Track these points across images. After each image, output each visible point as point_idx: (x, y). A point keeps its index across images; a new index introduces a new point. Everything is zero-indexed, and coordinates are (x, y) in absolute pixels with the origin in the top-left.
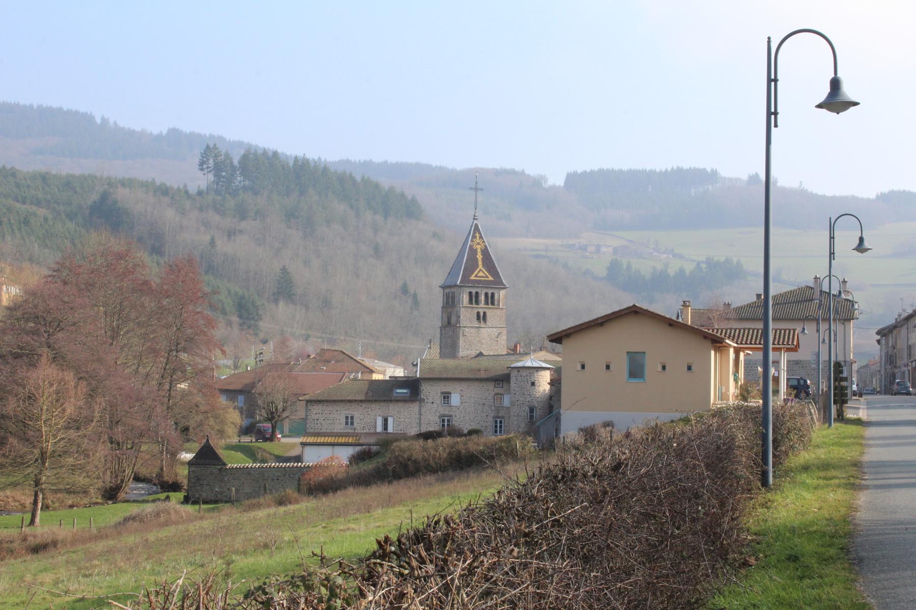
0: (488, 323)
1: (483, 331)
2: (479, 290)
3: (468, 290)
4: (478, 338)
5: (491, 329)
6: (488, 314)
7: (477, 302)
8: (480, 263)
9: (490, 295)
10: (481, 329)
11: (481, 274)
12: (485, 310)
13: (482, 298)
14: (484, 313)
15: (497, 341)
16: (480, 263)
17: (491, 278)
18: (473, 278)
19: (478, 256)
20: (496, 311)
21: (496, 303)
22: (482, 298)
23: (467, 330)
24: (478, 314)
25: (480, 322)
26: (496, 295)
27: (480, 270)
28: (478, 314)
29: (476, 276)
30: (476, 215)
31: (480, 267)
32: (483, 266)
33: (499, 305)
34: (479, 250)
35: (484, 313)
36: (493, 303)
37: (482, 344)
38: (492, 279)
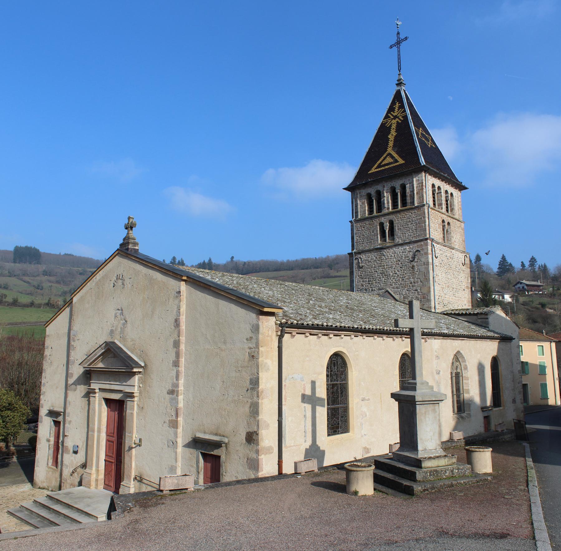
0: (398, 240)
1: (389, 253)
2: (379, 187)
3: (364, 192)
4: (381, 269)
5: (401, 249)
6: (395, 224)
7: (380, 207)
8: (391, 144)
9: (398, 191)
10: (385, 252)
11: (389, 160)
12: (391, 217)
13: (387, 199)
14: (391, 223)
15: (413, 267)
16: (391, 144)
17: (401, 161)
18: (373, 170)
19: (389, 137)
20: (408, 214)
21: (408, 199)
22: (387, 199)
23: (363, 256)
24: (382, 225)
25: (385, 241)
26: (408, 186)
27: (390, 155)
28: (382, 225)
29: (379, 166)
30: (402, 77)
31: (390, 150)
32: (394, 146)
33: (413, 203)
34: (394, 126)
35: (391, 223)
36: (404, 203)
37: (388, 276)
38: (404, 162)
